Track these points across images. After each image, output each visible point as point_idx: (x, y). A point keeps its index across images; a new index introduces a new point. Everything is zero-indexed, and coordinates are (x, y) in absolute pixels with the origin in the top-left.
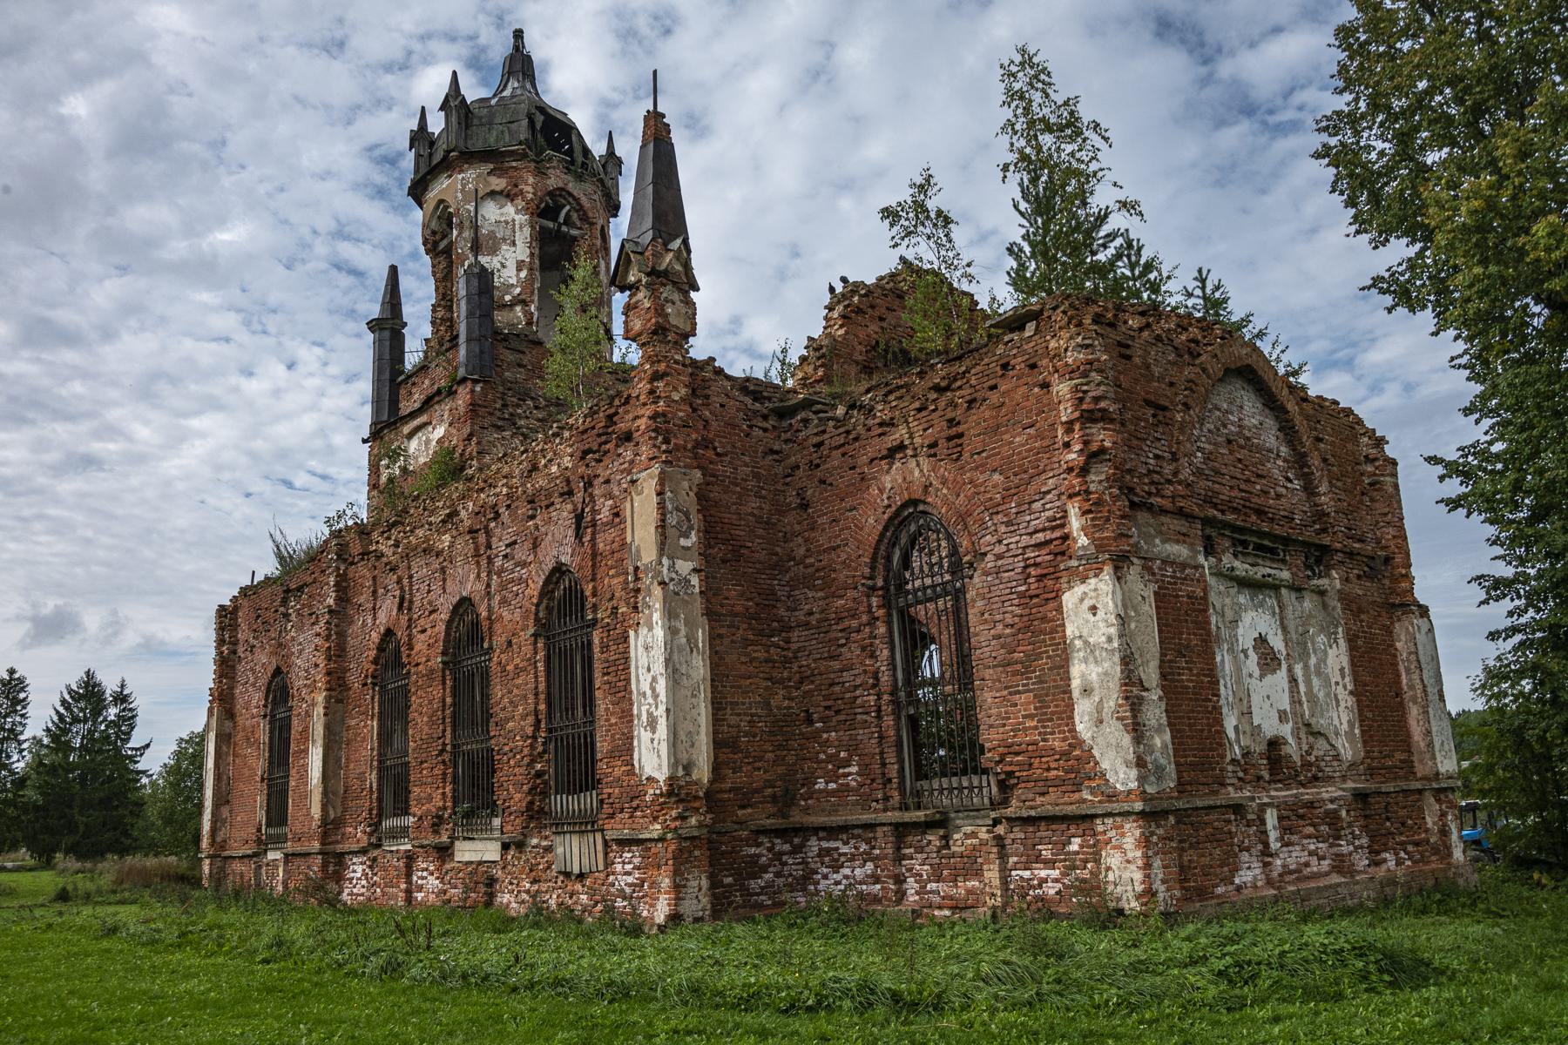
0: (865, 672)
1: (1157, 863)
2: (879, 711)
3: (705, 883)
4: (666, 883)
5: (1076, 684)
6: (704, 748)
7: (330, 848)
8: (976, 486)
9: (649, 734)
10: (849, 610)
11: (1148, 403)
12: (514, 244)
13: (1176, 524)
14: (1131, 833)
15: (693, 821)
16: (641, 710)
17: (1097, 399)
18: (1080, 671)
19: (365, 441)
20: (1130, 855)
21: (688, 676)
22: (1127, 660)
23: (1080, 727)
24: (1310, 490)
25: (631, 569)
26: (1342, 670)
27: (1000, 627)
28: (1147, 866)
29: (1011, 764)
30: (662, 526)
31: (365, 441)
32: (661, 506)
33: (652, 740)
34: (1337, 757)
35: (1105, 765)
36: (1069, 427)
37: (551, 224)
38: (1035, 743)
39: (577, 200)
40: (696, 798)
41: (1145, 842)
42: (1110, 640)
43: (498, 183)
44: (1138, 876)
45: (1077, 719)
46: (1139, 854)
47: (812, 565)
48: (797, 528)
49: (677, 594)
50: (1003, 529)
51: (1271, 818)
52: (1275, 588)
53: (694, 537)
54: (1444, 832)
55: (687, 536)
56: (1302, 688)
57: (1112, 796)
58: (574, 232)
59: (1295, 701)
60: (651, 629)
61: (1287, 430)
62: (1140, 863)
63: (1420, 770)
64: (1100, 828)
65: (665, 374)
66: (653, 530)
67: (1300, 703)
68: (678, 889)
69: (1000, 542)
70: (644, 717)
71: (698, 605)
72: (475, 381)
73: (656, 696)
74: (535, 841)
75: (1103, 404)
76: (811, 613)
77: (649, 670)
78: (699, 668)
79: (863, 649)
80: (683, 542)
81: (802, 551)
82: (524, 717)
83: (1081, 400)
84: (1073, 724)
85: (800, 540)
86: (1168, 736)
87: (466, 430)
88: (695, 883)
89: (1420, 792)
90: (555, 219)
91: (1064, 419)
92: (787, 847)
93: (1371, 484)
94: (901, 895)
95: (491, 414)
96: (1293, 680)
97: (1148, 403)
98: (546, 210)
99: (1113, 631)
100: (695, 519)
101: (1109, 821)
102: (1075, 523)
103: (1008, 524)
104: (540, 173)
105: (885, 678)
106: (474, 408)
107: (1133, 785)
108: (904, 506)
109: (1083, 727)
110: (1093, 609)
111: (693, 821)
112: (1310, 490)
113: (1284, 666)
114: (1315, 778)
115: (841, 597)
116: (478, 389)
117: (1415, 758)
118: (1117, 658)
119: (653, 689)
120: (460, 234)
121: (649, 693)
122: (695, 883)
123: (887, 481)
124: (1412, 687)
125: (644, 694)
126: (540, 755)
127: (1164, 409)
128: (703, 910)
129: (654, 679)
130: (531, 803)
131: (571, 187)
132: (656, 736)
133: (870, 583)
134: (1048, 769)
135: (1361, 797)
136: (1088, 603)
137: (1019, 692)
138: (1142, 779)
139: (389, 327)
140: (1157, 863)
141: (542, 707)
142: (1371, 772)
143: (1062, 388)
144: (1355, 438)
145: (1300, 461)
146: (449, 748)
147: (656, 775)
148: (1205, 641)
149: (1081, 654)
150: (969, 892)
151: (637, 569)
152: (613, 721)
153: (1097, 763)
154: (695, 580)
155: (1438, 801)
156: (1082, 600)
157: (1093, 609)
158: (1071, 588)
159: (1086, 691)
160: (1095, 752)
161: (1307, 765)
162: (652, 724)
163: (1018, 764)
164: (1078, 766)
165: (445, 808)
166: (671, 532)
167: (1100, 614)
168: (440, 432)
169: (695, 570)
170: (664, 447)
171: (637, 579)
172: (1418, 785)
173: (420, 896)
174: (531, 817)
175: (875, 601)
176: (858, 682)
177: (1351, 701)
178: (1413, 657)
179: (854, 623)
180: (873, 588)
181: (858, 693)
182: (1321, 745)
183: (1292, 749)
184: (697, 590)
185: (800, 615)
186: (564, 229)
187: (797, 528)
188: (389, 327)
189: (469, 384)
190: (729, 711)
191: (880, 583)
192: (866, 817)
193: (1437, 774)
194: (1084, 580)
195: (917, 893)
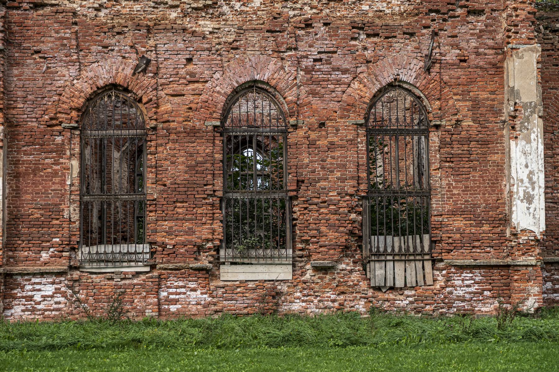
9: (525, 205)
33: (528, 209)
60: (529, 142)
66: (533, 83)
70: (521, 194)
73: (533, 183)
77: (527, 166)
119: (530, 179)
121: (526, 180)
125: (522, 181)
129: (531, 173)
132: (532, 206)
162: (529, 199)
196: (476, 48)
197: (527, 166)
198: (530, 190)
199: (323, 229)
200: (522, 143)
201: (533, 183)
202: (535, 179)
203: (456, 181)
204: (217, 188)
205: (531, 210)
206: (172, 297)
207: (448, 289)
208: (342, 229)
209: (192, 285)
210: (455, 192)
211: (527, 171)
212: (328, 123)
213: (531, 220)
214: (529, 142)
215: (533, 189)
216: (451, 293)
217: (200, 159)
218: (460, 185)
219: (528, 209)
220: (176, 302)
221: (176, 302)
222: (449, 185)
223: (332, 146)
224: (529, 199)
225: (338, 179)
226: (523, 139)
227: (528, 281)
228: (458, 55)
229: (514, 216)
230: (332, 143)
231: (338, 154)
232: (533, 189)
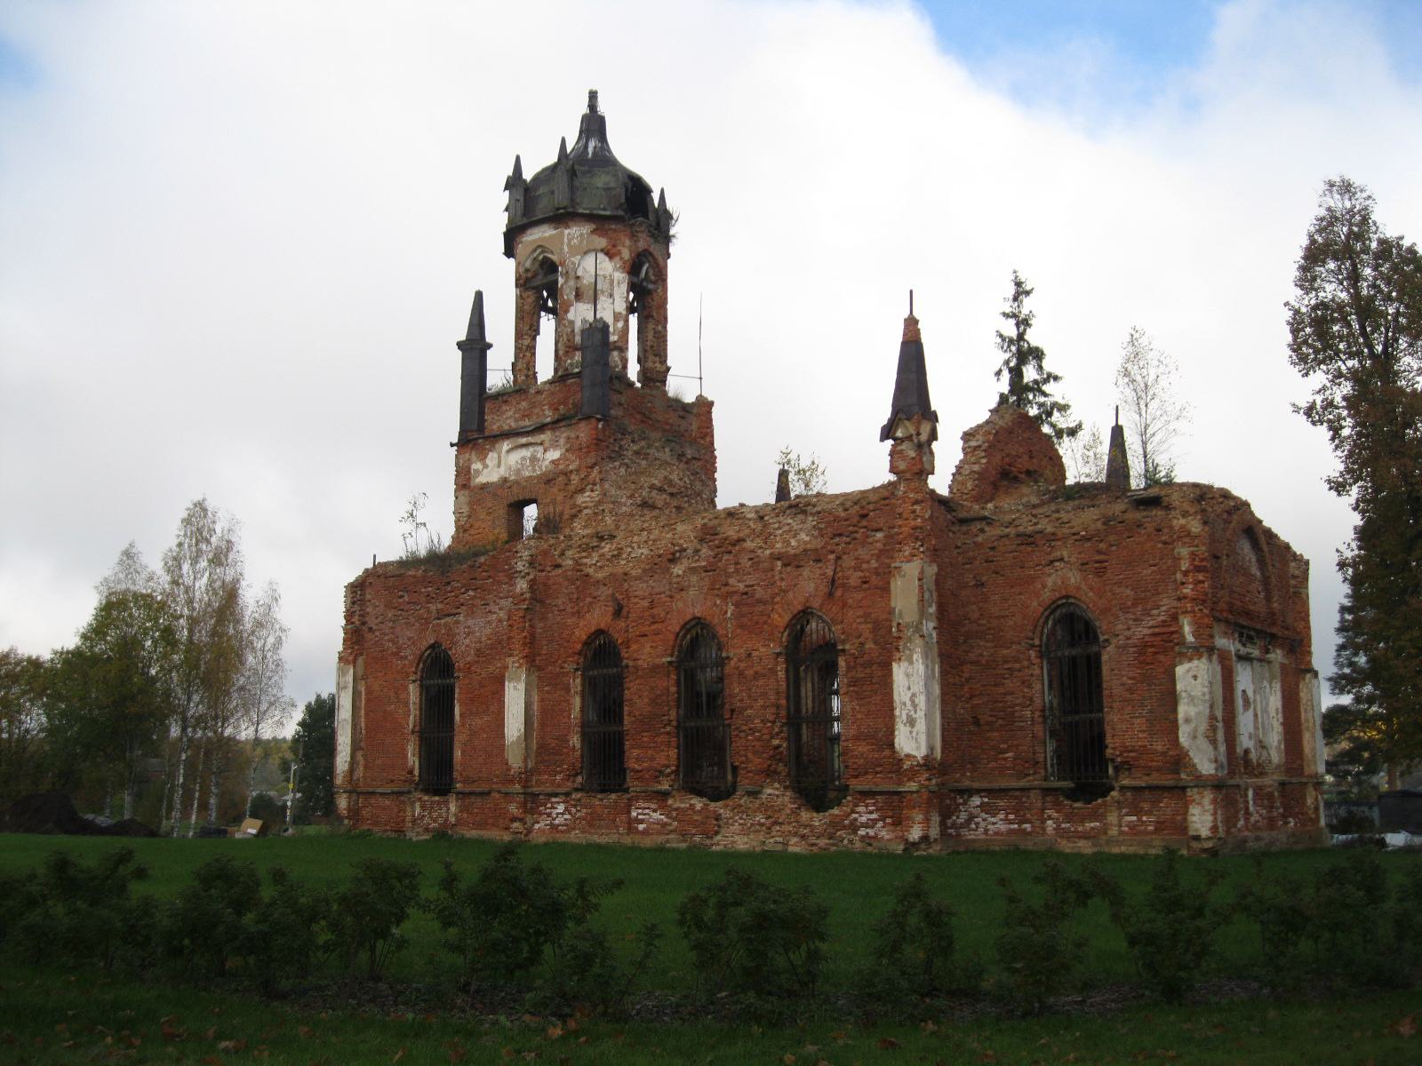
0: (1024, 697)
1: (1219, 812)
2: (1033, 720)
4: (920, 817)
5: (1181, 716)
7: (530, 790)
8: (1113, 594)
9: (908, 729)
10: (1013, 657)
12: (611, 296)
14: (1208, 797)
15: (934, 781)
16: (901, 714)
17: (1202, 560)
18: (1183, 710)
19: (452, 445)
20: (1207, 808)
22: (1212, 707)
23: (1182, 740)
24: (1268, 599)
25: (894, 624)
26: (1277, 709)
27: (1125, 679)
28: (1215, 814)
29: (1127, 757)
30: (922, 600)
31: (452, 445)
32: (921, 587)
33: (911, 732)
34: (1270, 761)
35: (1196, 761)
36: (1185, 573)
37: (635, 280)
38: (1145, 746)
39: (655, 259)
41: (1214, 802)
42: (1204, 695)
43: (602, 242)
44: (1210, 818)
45: (1180, 735)
46: (1212, 807)
47: (984, 625)
48: (973, 599)
50: (1131, 622)
51: (1250, 793)
54: (1317, 809)
55: (931, 606)
56: (1260, 720)
57: (1199, 777)
58: (651, 286)
59: (1256, 728)
60: (911, 663)
61: (1261, 563)
62: (1212, 812)
63: (1307, 771)
64: (1189, 794)
65: (922, 502)
68: (927, 820)
69: (1129, 629)
70: (904, 717)
72: (599, 420)
73: (915, 706)
74: (769, 791)
75: (1204, 563)
76: (981, 655)
77: (909, 688)
78: (937, 690)
79: (1023, 682)
81: (976, 615)
82: (764, 707)
83: (1194, 560)
84: (1178, 737)
85: (974, 607)
87: (590, 460)
89: (1306, 784)
90: (638, 276)
91: (1183, 569)
92: (961, 801)
93: (1294, 593)
94: (1044, 829)
95: (608, 447)
96: (1256, 715)
98: (633, 269)
99: (1206, 690)
101: (1195, 790)
102: (1187, 629)
103: (1135, 620)
104: (633, 236)
105: (1038, 701)
106: (598, 442)
107: (1213, 772)
108: (1060, 598)
109: (1184, 738)
110: (1195, 677)
111: (934, 781)
112: (1268, 599)
113: (1252, 706)
114: (1261, 774)
115: (1008, 648)
116: (600, 426)
117: (1305, 764)
118: (1207, 705)
119: (913, 702)
120: (566, 282)
121: (909, 703)
123: (1050, 582)
124: (1307, 721)
125: (905, 704)
126: (777, 734)
129: (914, 695)
130: (770, 766)
131: (651, 249)
132: (915, 730)
133: (1031, 642)
134: (1152, 761)
135: (1282, 784)
136: (1191, 674)
137: (1137, 717)
138: (1216, 769)
139: (475, 348)
140: (1219, 812)
141: (783, 702)
143: (1184, 552)
144: (1285, 564)
145: (1266, 581)
146: (674, 723)
147: (914, 753)
149: (1186, 701)
150: (1092, 828)
151: (899, 624)
152: (859, 716)
153: (1190, 759)
154: (934, 635)
155: (1315, 789)
156: (1188, 671)
157: (1195, 677)
158: (1181, 664)
159: (1187, 721)
160: (1191, 754)
162: (911, 722)
163: (1133, 757)
164: (1179, 760)
165: (668, 766)
166: (926, 604)
167: (1199, 680)
168: (554, 454)
169: (934, 628)
170: (921, 549)
171: (899, 630)
172: (1305, 780)
173: (641, 827)
174: (768, 775)
175: (1032, 653)
176: (1018, 701)
177: (1280, 729)
178: (1309, 703)
179: (1017, 666)
180: (1033, 646)
181: (1017, 708)
182: (1265, 753)
183: (1253, 756)
185: (972, 656)
186: (645, 284)
187: (973, 599)
188: (475, 348)
189: (593, 420)
191: (1037, 642)
192: (1022, 784)
193: (1317, 773)
194: (1190, 660)
195: (1054, 829)
196: (876, 568)
197: (909, 688)
198: (912, 712)
199: (750, 755)
200: (904, 664)
201: (915, 706)
202: (917, 701)
203: (859, 705)
204: (672, 718)
205: (914, 734)
206: (640, 817)
207: (854, 815)
208: (765, 755)
209: (653, 806)
210: (859, 716)
211: (909, 694)
212: (755, 654)
213: (914, 745)
214: (911, 663)
215: (915, 712)
216: (856, 819)
217: (659, 692)
218: (863, 709)
219: (911, 732)
220: (642, 822)
221: (642, 822)
222: (853, 709)
223: (757, 675)
224: (911, 722)
225: (762, 706)
226: (906, 660)
227: (914, 808)
228: (860, 578)
229: (896, 741)
230: (756, 673)
231: (761, 682)
232: (915, 712)
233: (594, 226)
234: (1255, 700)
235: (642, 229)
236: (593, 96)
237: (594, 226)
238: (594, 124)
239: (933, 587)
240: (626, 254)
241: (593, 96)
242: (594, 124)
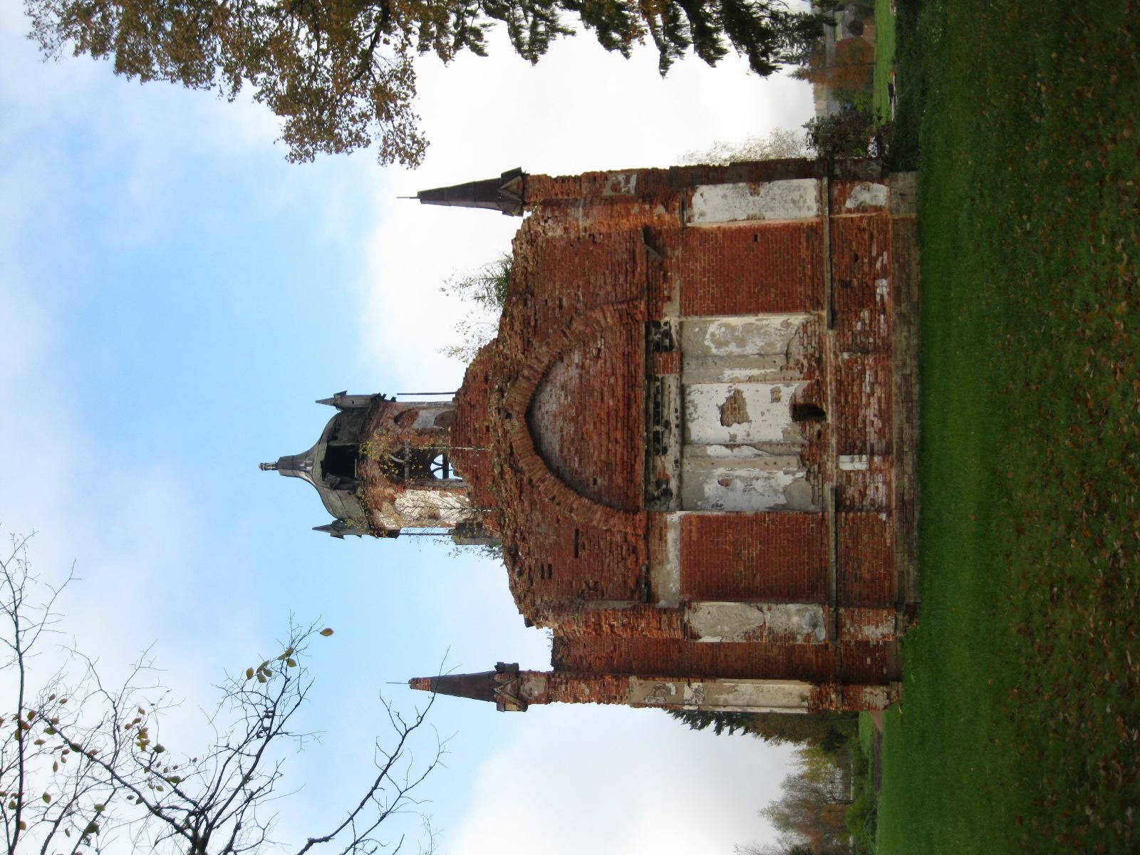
3: (868, 689)
6: (792, 686)
11: (576, 555)
13: (654, 542)
21: (751, 694)
40: (820, 692)
49: (704, 699)
52: (683, 391)
53: (670, 685)
55: (669, 690)
67: (766, 375)
71: (710, 684)
80: (673, 693)
86: (792, 607)
88: (868, 696)
96: (750, 379)
97: (576, 555)
100: (659, 682)
122: (868, 696)
127: (577, 531)
128: (883, 692)
142: (817, 304)
148: (730, 523)
154: (695, 685)
161: (809, 375)
169: (689, 685)
184: (701, 684)
190: (770, 654)
233: (375, 511)
234: (732, 381)
235: (363, 471)
236: (264, 467)
237: (375, 511)
238: (289, 466)
239: (651, 683)
240: (390, 491)
241: (264, 467)
242: (289, 466)
